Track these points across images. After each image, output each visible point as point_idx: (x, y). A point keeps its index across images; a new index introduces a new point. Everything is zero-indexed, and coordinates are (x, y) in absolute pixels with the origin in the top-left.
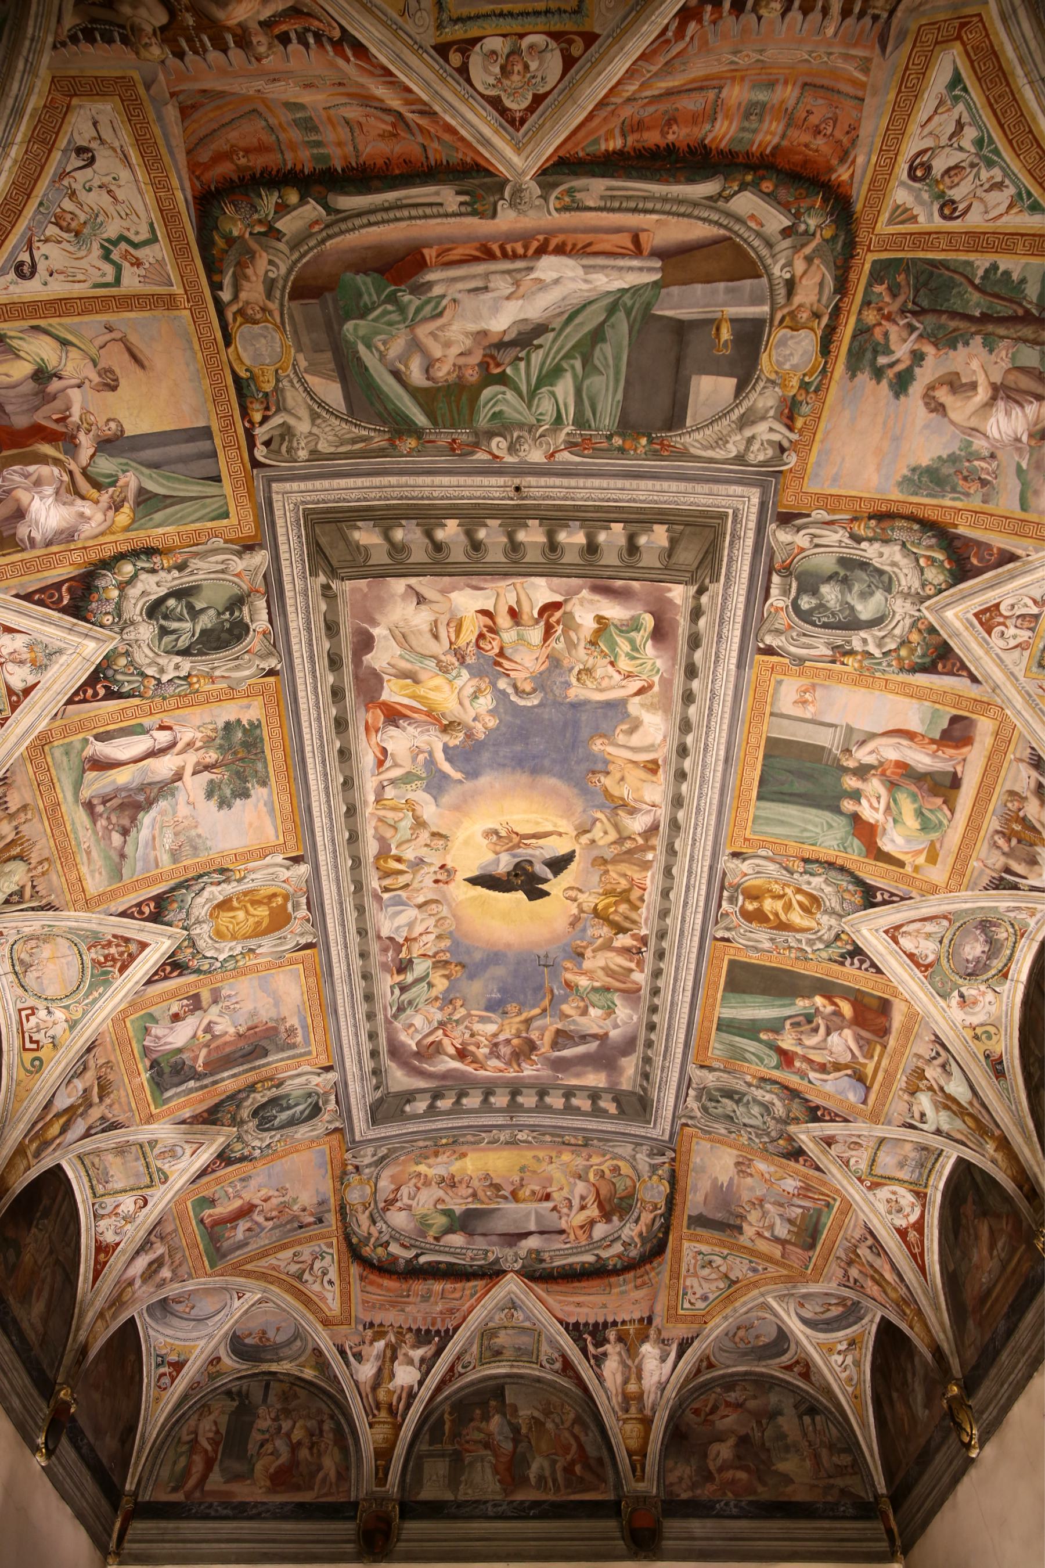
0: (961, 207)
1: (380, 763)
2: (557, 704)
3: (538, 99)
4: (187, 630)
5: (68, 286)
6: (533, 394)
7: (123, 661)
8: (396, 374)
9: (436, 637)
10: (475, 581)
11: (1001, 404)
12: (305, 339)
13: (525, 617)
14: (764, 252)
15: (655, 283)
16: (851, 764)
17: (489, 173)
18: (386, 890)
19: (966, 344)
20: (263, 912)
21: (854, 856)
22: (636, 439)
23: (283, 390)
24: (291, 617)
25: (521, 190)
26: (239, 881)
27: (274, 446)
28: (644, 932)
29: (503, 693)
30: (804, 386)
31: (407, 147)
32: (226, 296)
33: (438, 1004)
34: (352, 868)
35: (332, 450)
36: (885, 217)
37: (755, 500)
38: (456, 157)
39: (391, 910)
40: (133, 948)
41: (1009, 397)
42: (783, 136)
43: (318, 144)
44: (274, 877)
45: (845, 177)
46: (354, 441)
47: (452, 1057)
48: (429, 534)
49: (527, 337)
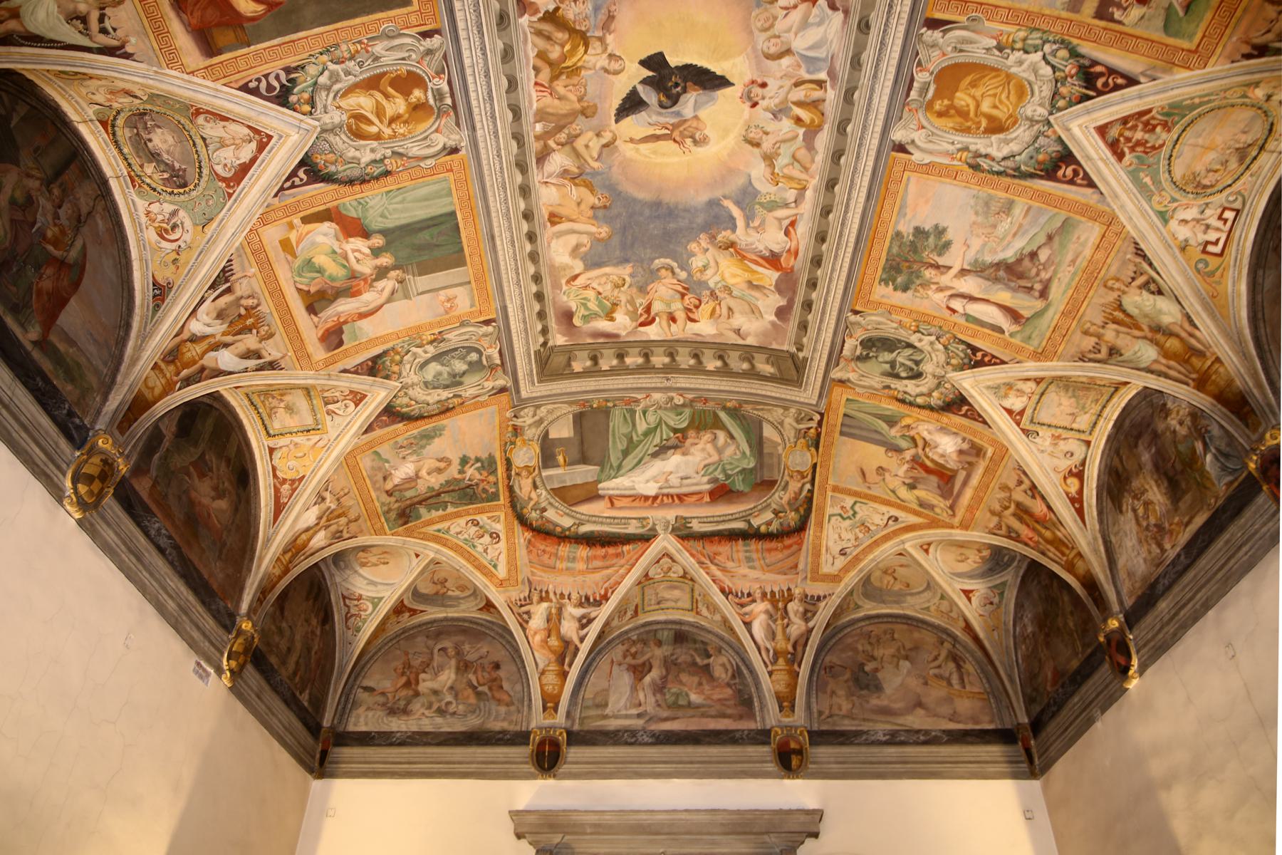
1: (793, 224)
2: (642, 261)
4: (902, 357)
6: (659, 424)
7: (954, 361)
8: (732, 437)
9: (730, 309)
10: (699, 339)
11: (412, 474)
12: (775, 460)
13: (665, 317)
16: (393, 274)
18: (820, 84)
20: (962, 99)
21: (348, 201)
24: (829, 341)
26: (966, 149)
29: (682, 269)
30: (513, 443)
32: (808, 486)
34: (848, 121)
36: (502, 518)
38: (692, 542)
39: (821, 53)
40: (1114, 132)
44: (931, 137)
48: (726, 364)
49: (661, 451)
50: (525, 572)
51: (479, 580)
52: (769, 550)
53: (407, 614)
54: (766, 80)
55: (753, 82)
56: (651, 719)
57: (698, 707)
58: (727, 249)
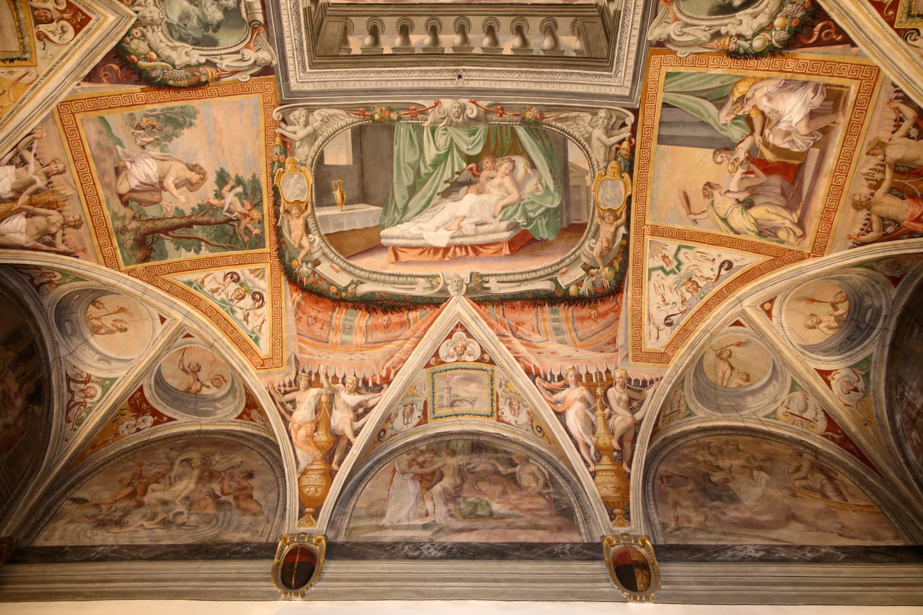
0: (228, 279)
3: (450, 336)
5: (707, 251)
6: (450, 150)
8: (533, 166)
11: (155, 180)
12: (583, 195)
14: (326, 250)
15: (383, 228)
17: (473, 300)
19: (193, 209)
22: (381, 118)
23: (605, 161)
25: (458, 290)
27: (621, 122)
30: (282, 165)
31: (513, 316)
35: (582, 114)
36: (268, 272)
41: (152, 185)
42: (332, 317)
43: (555, 320)
45: (295, 295)
46: (566, 119)
49: (454, 188)
50: (291, 347)
51: (237, 358)
52: (582, 319)
53: (150, 419)
56: (440, 530)
57: (502, 517)
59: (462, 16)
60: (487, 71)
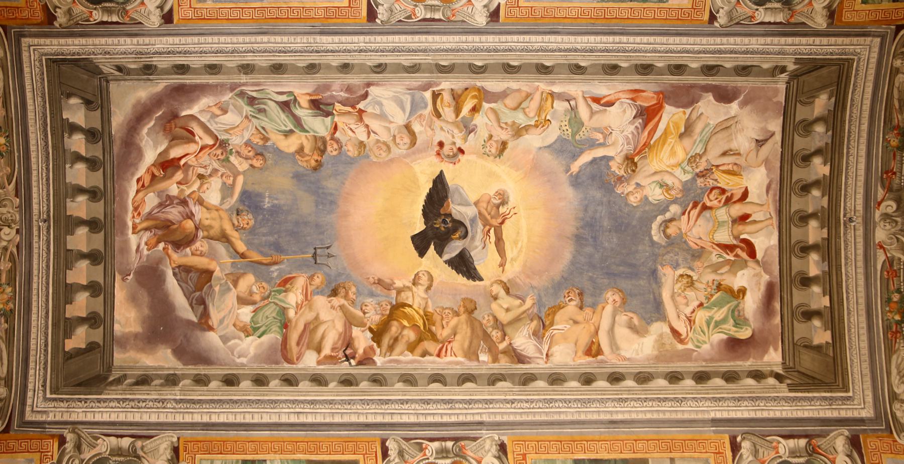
9: (724, 154)
10: (775, 186)
28: (379, 360)
33: (257, 140)
37: (864, 414)
47: (166, 151)
48: (818, 152)
54: (436, 143)
55: (438, 154)
58: (635, 164)
59: (790, 219)
60: (846, 191)
